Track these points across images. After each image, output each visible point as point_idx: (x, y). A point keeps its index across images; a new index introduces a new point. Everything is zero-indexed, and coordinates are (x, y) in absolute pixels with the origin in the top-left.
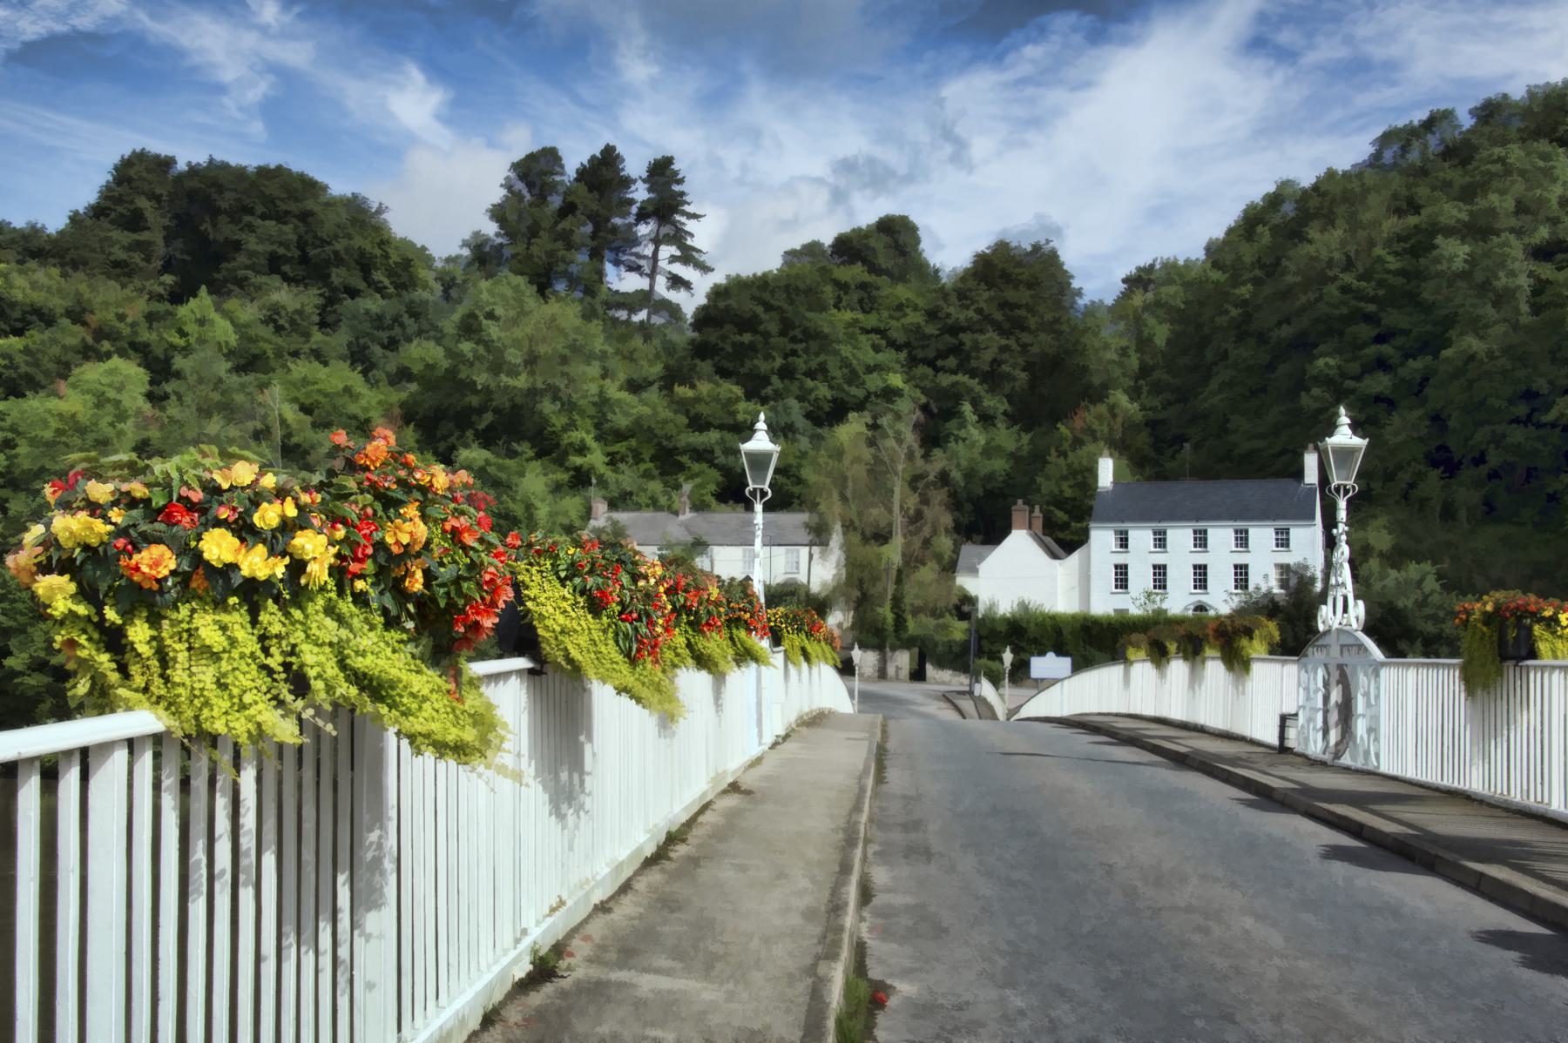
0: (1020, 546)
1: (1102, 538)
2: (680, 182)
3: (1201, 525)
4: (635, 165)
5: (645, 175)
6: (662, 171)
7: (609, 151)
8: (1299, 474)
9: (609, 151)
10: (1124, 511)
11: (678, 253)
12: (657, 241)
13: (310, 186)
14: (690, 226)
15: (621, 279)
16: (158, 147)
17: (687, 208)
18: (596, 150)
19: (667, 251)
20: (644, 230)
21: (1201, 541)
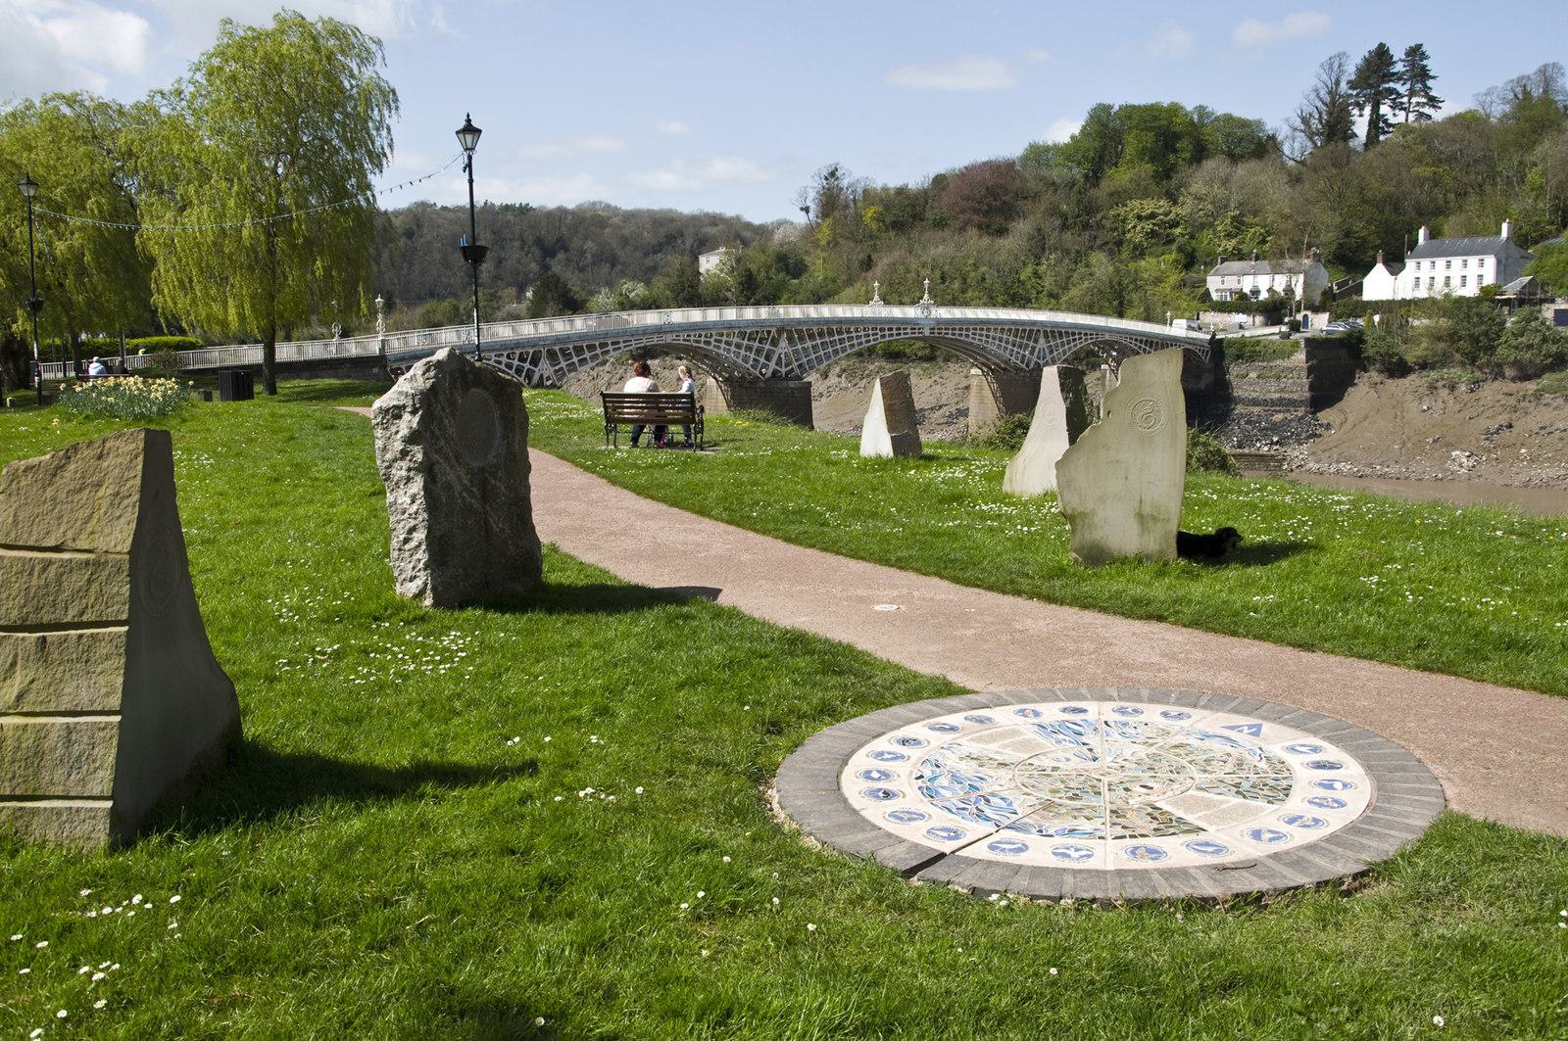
0: (1379, 270)
1: (1410, 264)
2: (1427, 58)
3: (1449, 259)
4: (1398, 52)
5: (1403, 57)
6: (1416, 53)
7: (1381, 46)
8: (1499, 232)
9: (1381, 46)
10: (1432, 253)
11: (1424, 100)
12: (1412, 93)
13: (1174, 110)
14: (1430, 83)
15: (1394, 115)
16: (1106, 101)
17: (1431, 74)
18: (1374, 46)
19: (1414, 100)
20: (1402, 88)
21: (1448, 265)
